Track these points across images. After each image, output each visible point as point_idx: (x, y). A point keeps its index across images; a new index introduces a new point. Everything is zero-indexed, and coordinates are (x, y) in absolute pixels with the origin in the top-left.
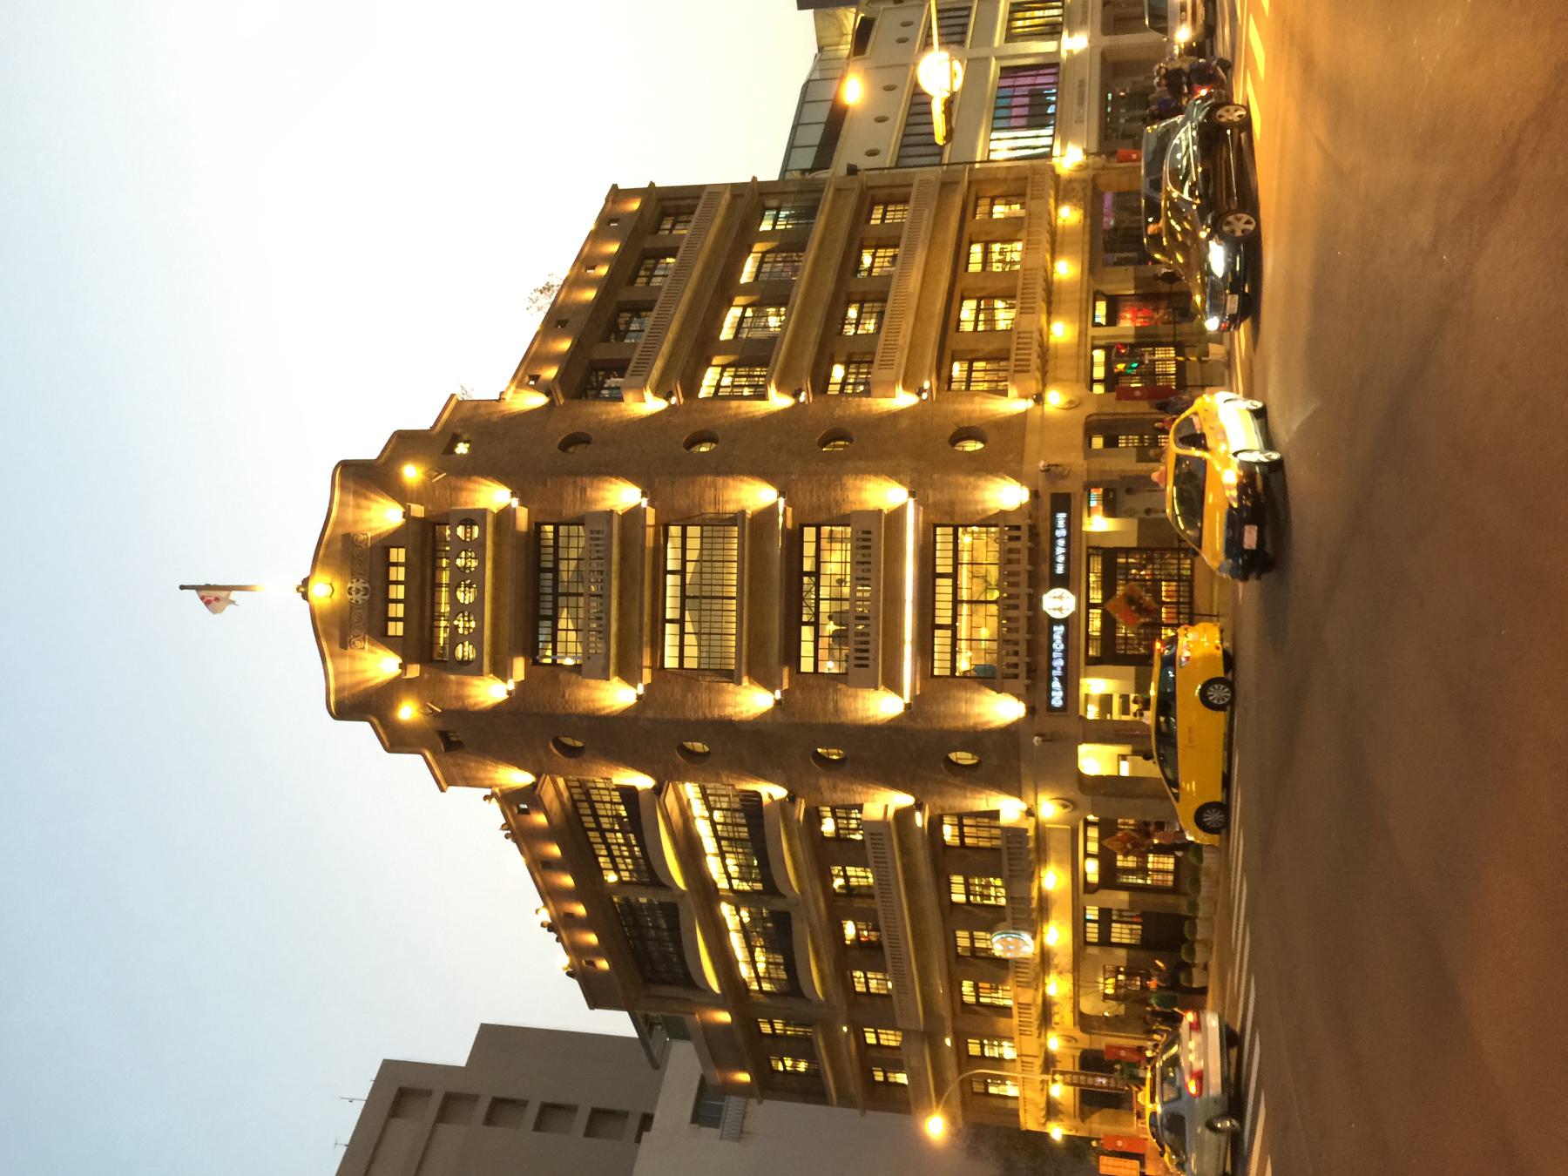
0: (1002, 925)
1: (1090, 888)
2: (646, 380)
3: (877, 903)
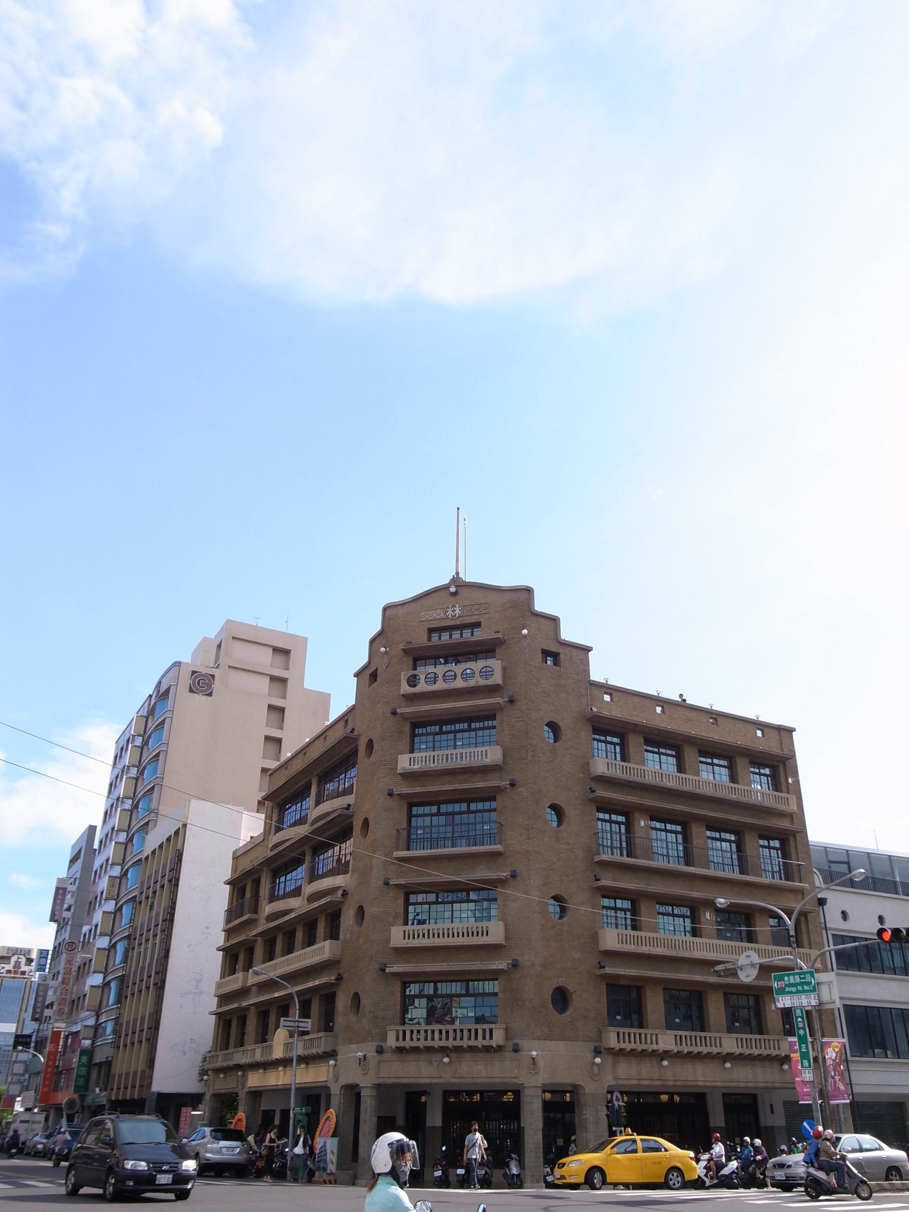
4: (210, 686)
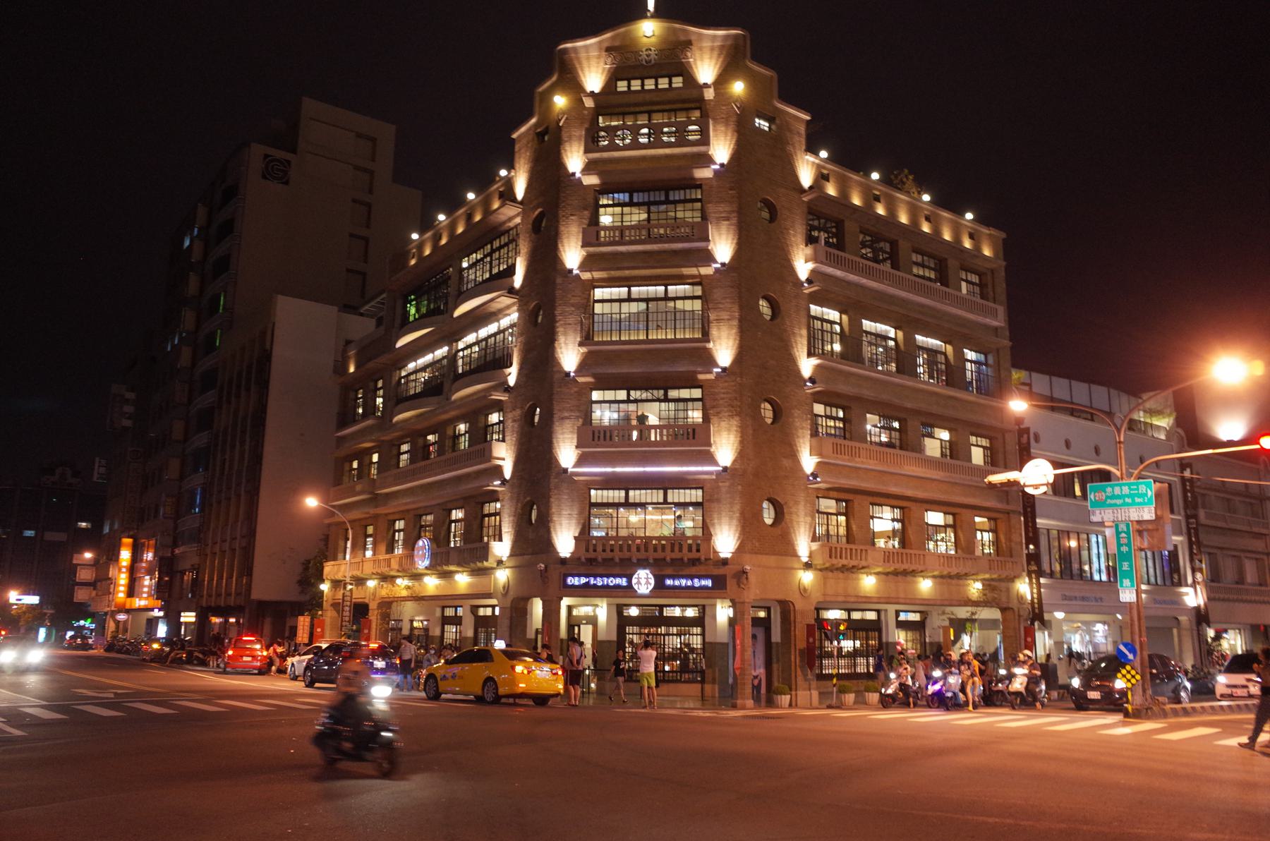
0: (435, 546)
1: (475, 609)
2: (822, 263)
3: (449, 455)
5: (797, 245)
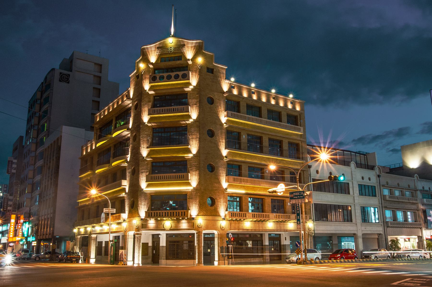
2: (230, 117)
4: (68, 79)
5: (221, 111)
